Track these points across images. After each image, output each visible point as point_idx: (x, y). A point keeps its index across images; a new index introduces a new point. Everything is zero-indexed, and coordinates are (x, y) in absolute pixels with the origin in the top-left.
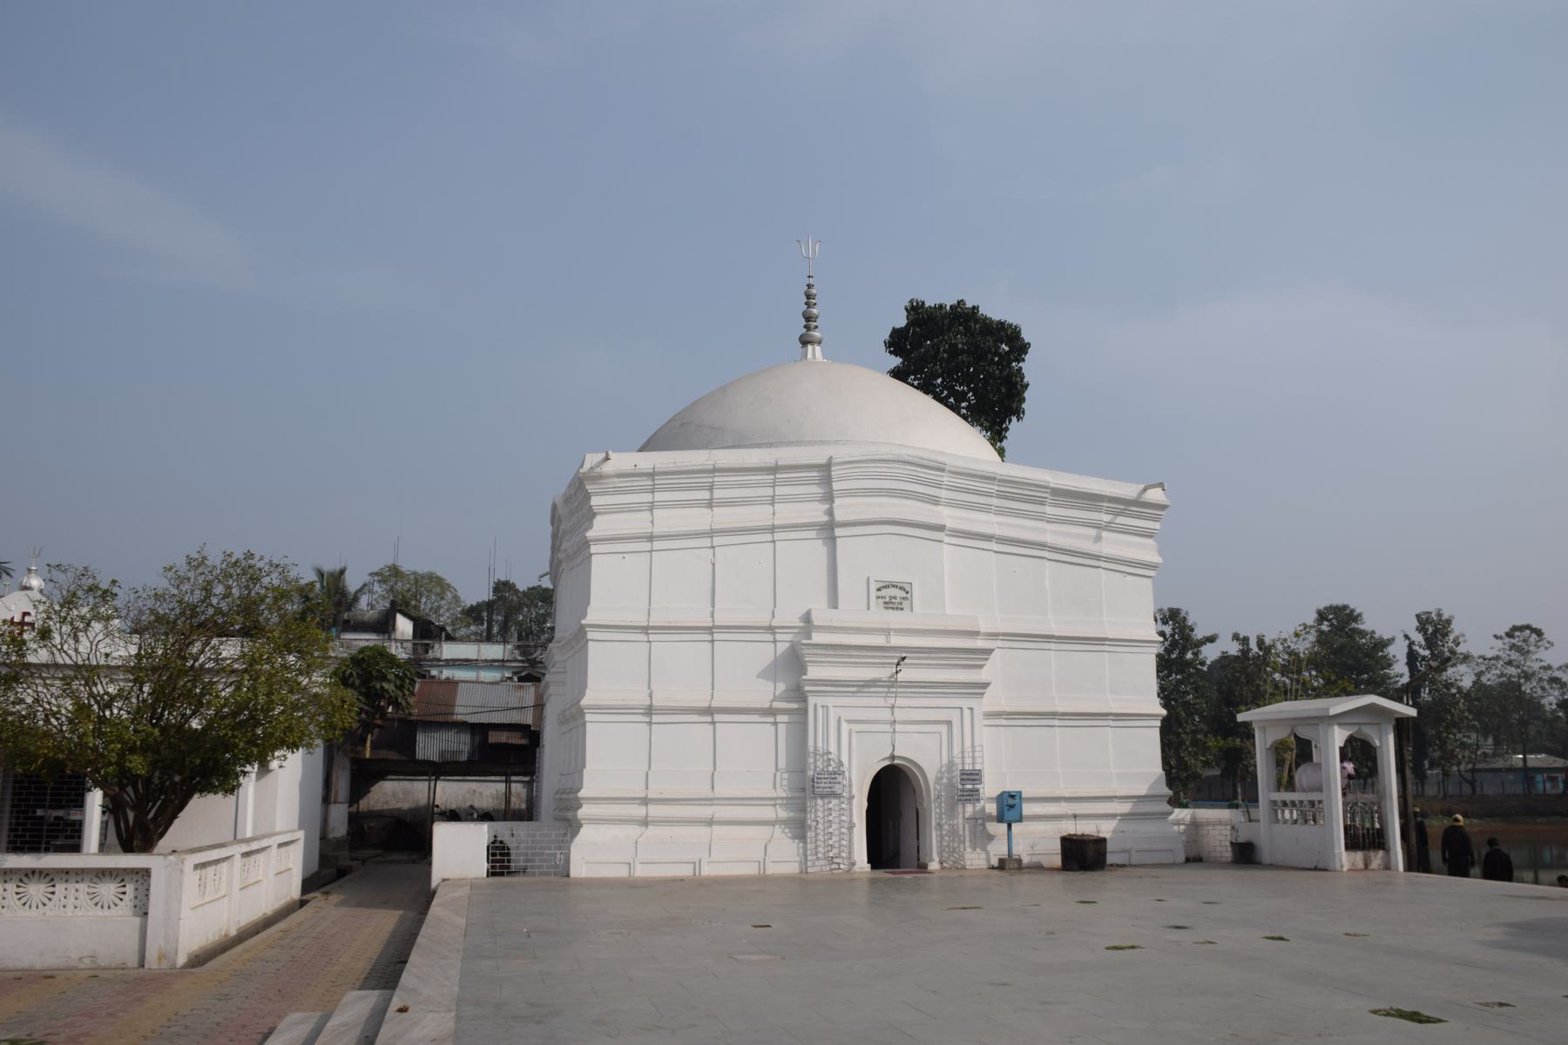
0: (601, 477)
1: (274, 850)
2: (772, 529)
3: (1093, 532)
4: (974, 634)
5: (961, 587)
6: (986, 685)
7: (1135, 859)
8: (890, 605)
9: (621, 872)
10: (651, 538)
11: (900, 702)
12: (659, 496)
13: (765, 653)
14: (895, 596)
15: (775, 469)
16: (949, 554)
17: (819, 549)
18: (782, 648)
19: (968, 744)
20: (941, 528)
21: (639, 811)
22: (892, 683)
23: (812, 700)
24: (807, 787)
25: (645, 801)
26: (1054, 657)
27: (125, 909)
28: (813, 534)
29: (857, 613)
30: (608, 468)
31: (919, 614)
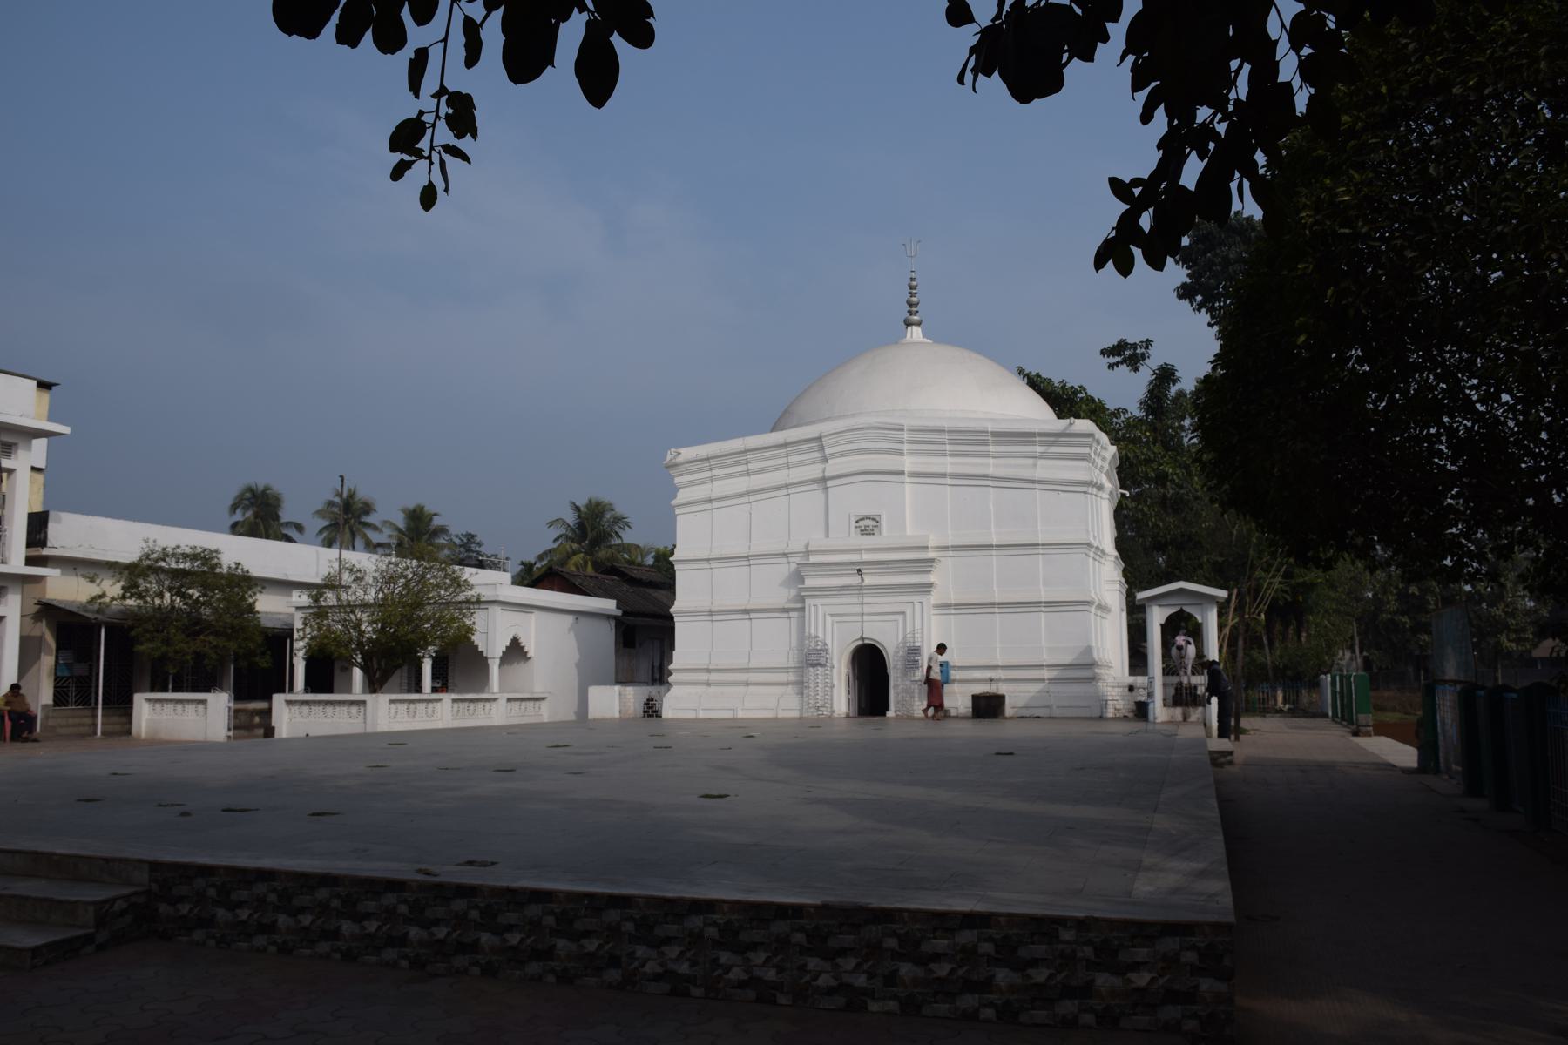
0: (676, 465)
1: (502, 702)
2: (787, 486)
3: (1031, 461)
4: (926, 548)
5: (913, 515)
6: (931, 585)
7: (1057, 713)
8: (865, 532)
9: (690, 715)
10: (711, 501)
11: (866, 600)
12: (715, 472)
13: (784, 570)
14: (868, 525)
15: (785, 445)
16: (909, 489)
17: (820, 495)
18: (793, 566)
19: (918, 626)
20: (902, 473)
21: (704, 677)
22: (860, 588)
23: (808, 602)
24: (812, 658)
25: (708, 671)
26: (995, 561)
27: (360, 719)
28: (815, 486)
29: (845, 540)
30: (680, 459)
31: (886, 536)
